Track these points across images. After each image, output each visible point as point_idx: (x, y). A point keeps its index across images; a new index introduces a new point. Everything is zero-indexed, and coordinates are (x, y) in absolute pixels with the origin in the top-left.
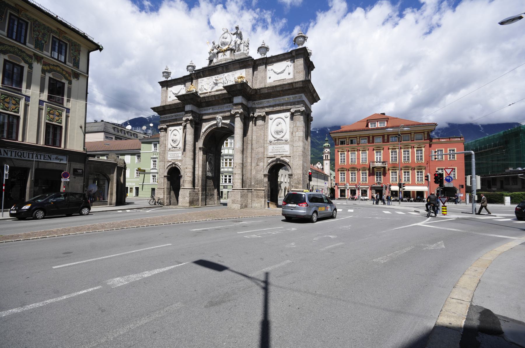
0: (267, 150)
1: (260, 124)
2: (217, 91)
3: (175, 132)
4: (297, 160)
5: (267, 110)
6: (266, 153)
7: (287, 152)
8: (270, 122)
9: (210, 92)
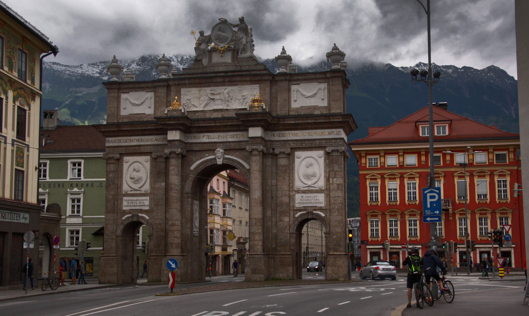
1: (282, 163)
3: (136, 165)
4: (336, 214)
5: (292, 145)
6: (291, 205)
7: (321, 203)
8: (297, 161)
9: (202, 111)
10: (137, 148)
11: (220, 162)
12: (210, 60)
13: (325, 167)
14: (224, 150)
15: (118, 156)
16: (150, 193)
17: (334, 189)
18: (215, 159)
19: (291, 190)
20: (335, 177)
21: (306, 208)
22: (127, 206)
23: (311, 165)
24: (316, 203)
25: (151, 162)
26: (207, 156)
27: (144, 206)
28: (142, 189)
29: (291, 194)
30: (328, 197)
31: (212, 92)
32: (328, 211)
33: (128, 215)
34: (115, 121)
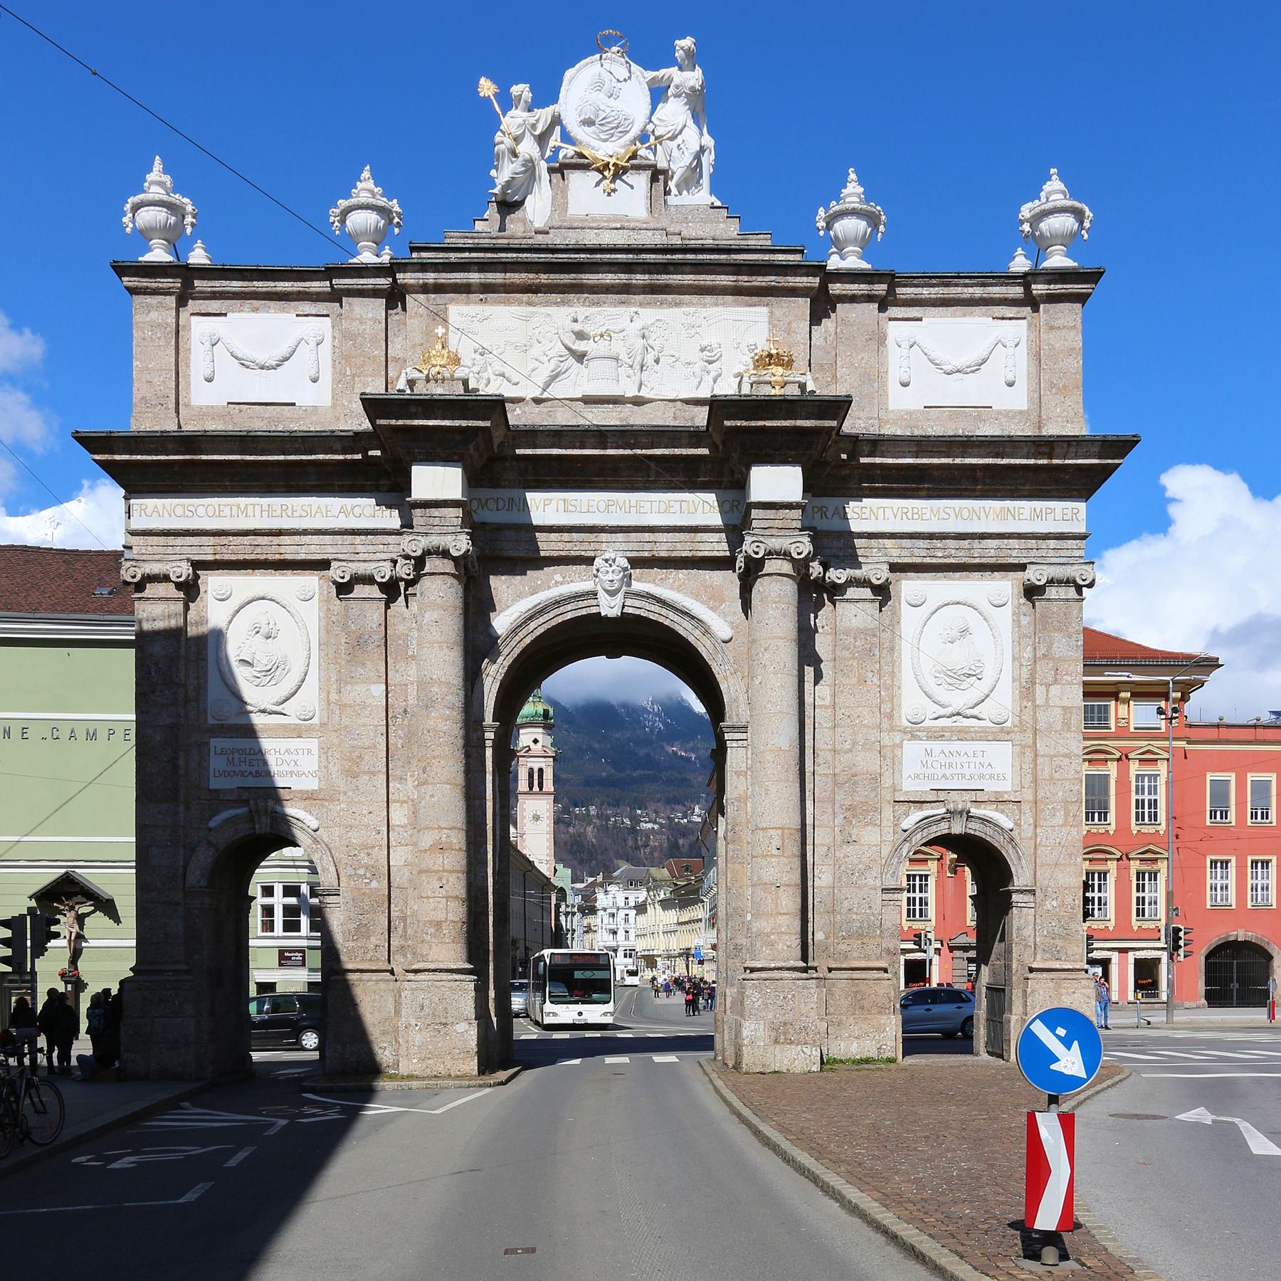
0: (896, 763)
1: (855, 623)
2: (589, 400)
4: (1059, 820)
6: (887, 781)
9: (538, 401)
12: (560, 201)
13: (1018, 640)
14: (630, 560)
15: (185, 570)
16: (323, 725)
17: (1050, 728)
18: (594, 594)
19: (885, 725)
20: (1056, 682)
21: (942, 796)
22: (226, 774)
23: (964, 632)
24: (982, 777)
27: (298, 775)
28: (286, 708)
29: (886, 739)
30: (1030, 753)
31: (577, 327)
32: (1025, 807)
33: (232, 812)
34: (171, 426)
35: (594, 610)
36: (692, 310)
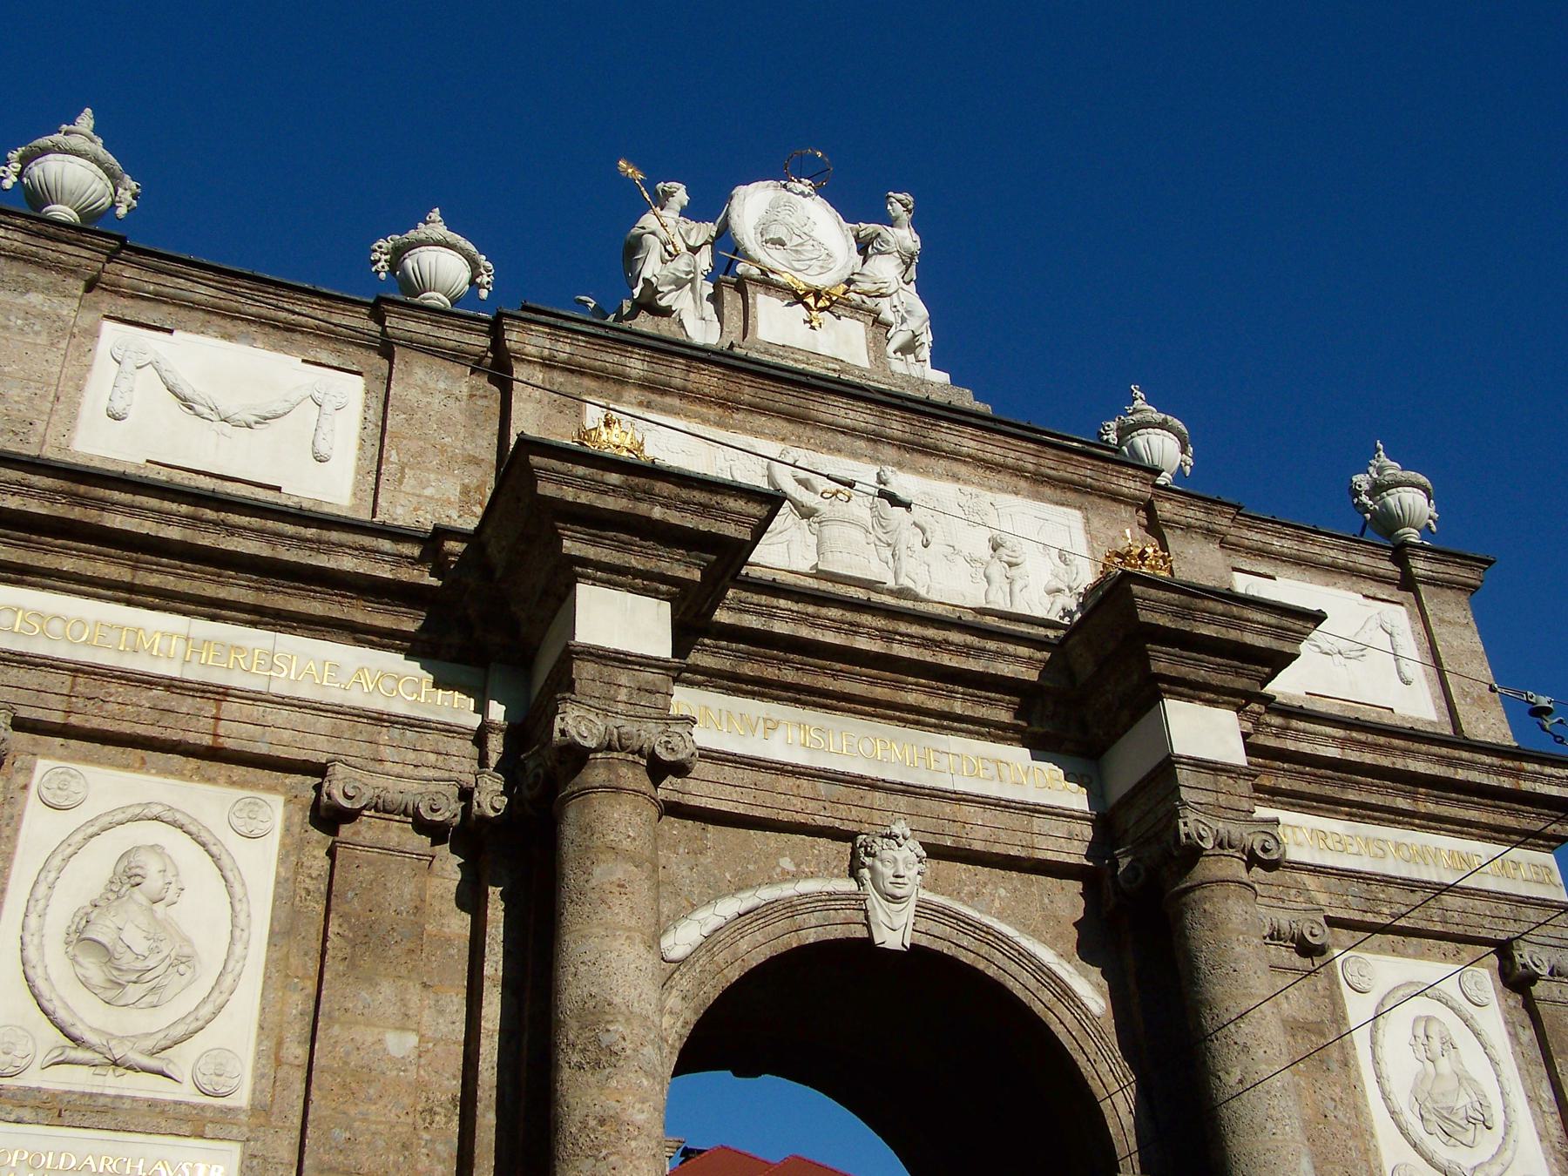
10: (186, 704)
11: (894, 930)
18: (858, 902)
25: (291, 850)
26: (788, 877)
35: (860, 932)
36: (968, 489)
